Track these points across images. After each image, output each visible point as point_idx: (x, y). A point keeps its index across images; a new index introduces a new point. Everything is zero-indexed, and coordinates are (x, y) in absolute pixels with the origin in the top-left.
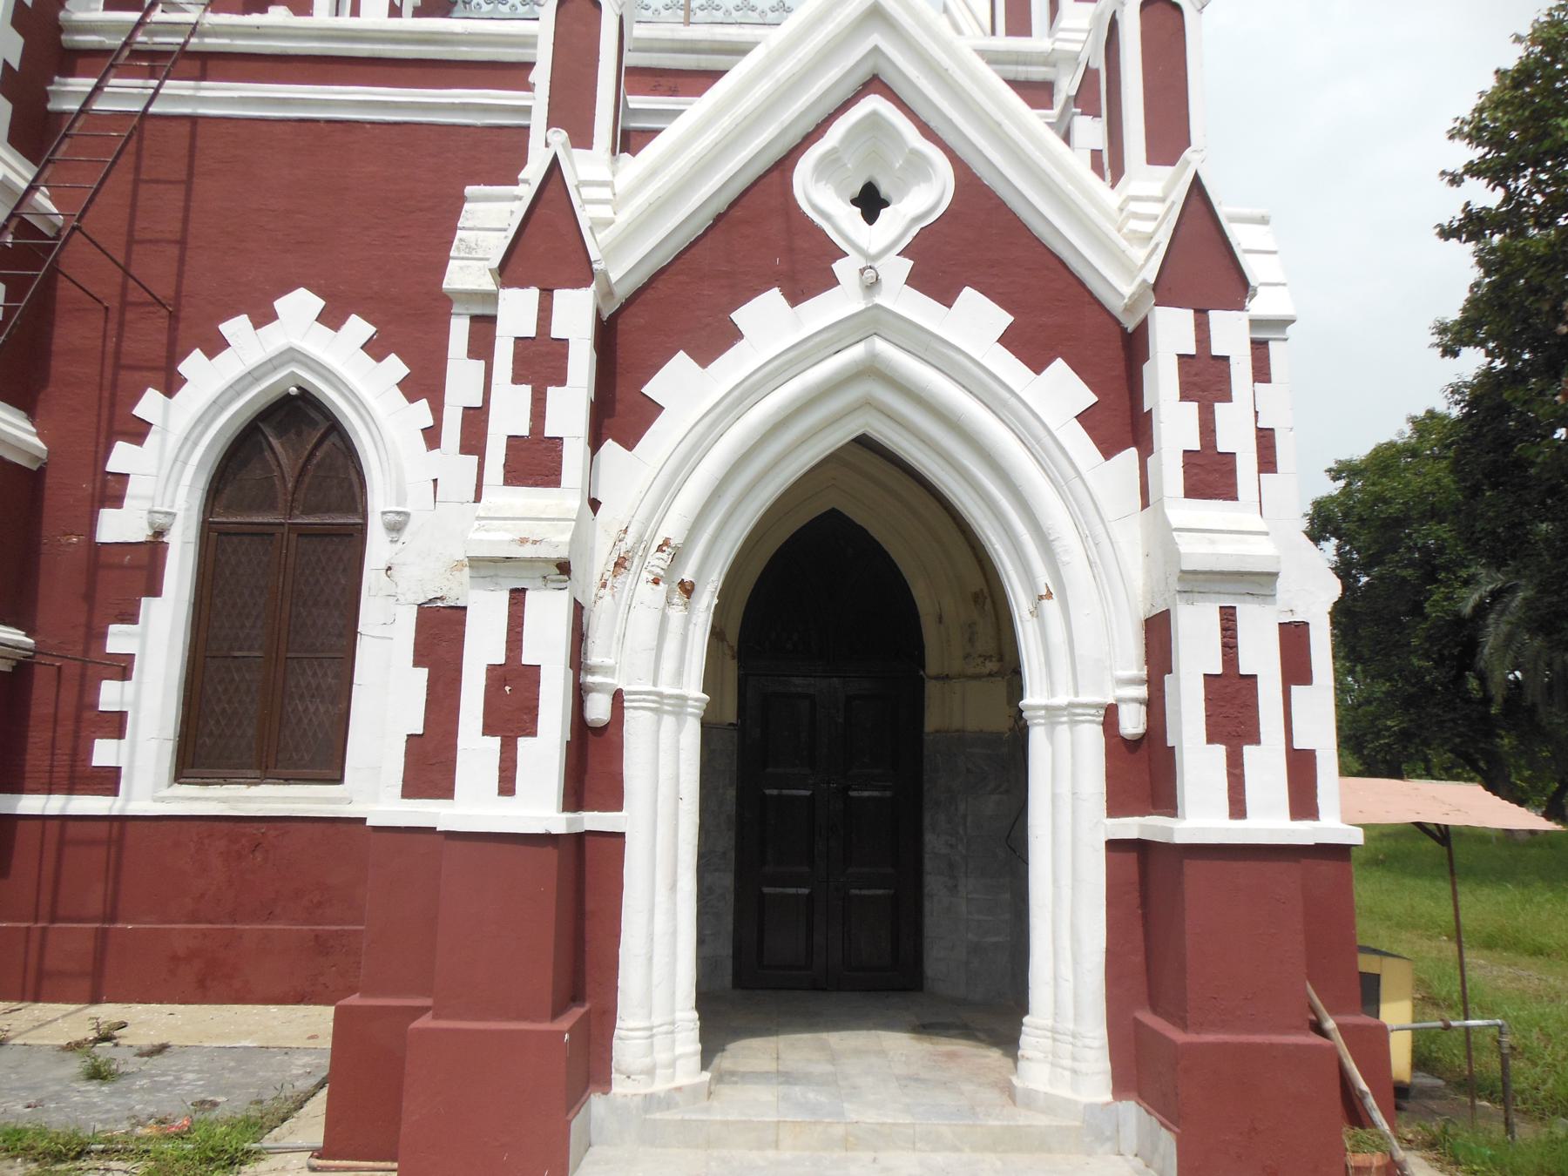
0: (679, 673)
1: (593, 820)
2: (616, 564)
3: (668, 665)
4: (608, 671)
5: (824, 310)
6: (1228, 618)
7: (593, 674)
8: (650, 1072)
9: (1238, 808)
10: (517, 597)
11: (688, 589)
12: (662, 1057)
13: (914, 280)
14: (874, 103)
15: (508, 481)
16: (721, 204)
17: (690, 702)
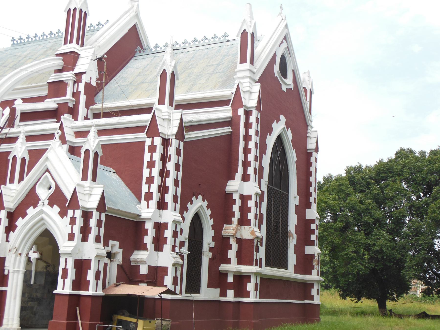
0: (19, 267)
2: (9, 251)
4: (7, 267)
6: (66, 259)
7: (6, 267)
8: (8, 325)
9: (63, 289)
11: (20, 254)
12: (10, 323)
13: (49, 204)
14: (47, 174)
17: (21, 271)
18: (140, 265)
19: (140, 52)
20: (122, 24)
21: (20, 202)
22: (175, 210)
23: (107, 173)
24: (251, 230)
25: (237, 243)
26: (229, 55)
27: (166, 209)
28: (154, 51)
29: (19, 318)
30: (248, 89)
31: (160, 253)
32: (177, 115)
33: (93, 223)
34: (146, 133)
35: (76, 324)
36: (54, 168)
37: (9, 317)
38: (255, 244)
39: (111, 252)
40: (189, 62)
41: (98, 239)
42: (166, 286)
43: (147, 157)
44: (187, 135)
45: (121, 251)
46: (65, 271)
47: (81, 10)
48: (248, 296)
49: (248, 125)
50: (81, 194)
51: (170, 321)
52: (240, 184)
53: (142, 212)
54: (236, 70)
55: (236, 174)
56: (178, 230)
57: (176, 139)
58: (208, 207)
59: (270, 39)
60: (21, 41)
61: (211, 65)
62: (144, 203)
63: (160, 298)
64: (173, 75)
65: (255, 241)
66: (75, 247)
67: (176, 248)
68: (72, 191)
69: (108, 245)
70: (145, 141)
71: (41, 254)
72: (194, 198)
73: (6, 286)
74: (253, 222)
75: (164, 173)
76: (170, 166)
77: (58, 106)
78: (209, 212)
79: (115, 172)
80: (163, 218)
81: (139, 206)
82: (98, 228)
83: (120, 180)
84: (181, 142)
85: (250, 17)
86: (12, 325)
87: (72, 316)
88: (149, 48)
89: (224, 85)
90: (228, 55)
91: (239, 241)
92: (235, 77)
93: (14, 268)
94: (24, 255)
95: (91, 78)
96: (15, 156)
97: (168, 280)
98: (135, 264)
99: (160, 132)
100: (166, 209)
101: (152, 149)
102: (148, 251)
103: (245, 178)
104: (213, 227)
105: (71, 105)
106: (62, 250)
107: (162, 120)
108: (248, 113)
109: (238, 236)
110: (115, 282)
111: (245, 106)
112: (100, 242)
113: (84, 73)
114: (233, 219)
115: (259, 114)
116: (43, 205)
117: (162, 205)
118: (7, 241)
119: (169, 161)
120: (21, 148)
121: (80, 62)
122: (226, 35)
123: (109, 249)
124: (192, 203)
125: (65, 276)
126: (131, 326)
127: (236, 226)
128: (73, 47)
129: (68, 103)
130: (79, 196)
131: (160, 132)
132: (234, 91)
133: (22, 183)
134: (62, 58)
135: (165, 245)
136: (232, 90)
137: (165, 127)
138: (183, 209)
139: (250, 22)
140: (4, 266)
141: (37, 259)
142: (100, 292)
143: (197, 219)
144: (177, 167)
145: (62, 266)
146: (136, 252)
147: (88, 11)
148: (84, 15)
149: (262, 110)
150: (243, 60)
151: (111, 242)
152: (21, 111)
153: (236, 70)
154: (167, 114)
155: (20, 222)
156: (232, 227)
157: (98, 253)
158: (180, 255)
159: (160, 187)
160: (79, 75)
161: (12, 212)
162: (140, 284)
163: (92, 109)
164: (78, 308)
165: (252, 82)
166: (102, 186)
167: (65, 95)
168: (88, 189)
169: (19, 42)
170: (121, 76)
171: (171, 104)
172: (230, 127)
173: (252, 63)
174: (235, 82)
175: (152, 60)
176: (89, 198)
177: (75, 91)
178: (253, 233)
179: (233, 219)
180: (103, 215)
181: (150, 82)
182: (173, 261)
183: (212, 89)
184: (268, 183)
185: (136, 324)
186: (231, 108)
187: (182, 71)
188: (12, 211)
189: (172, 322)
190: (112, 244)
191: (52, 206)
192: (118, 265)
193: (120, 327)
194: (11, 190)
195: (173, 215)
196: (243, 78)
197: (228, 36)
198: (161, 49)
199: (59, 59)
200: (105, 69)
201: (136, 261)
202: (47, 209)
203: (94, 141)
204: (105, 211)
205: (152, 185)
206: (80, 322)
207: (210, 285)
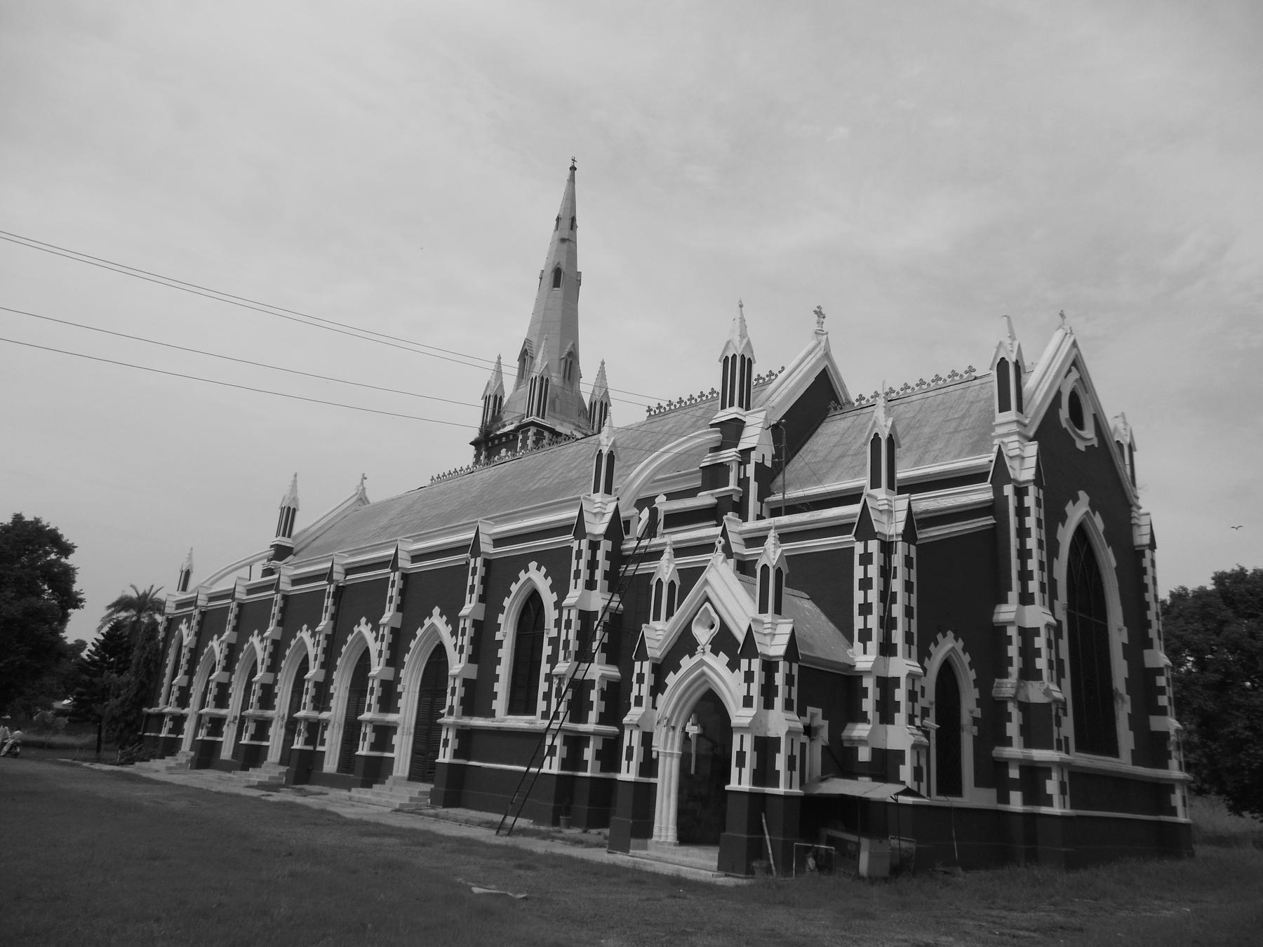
0: (672, 747)
1: (652, 780)
3: (669, 745)
5: (696, 659)
6: (742, 737)
8: (660, 836)
9: (740, 783)
10: (631, 731)
11: (674, 728)
12: (663, 833)
14: (707, 605)
15: (635, 706)
16: (679, 634)
18: (857, 748)
19: (835, 409)
20: (805, 369)
21: (669, 648)
22: (910, 657)
23: (796, 600)
24: (1044, 688)
25: (1020, 710)
26: (980, 401)
27: (895, 655)
28: (857, 406)
29: (675, 827)
30: (1017, 452)
31: (889, 726)
32: (901, 503)
33: (779, 679)
34: (855, 535)
35: (763, 840)
36: (717, 595)
37: (661, 824)
38: (1054, 713)
39: (812, 725)
40: (914, 417)
41: (788, 706)
42: (903, 783)
43: (858, 572)
44: (921, 533)
45: (826, 723)
46: (741, 755)
47: (743, 357)
48: (1050, 804)
49: (1022, 512)
50: (758, 635)
51: (913, 842)
52: (1018, 609)
53: (856, 660)
54: (994, 423)
55: (1009, 593)
56: (918, 689)
57: (902, 541)
58: (965, 650)
59: (1048, 367)
60: (660, 411)
61: (951, 419)
62: (858, 645)
63: (894, 801)
64: (891, 442)
65: (1054, 707)
66: (755, 717)
67: (916, 719)
68: (745, 629)
69: (805, 715)
70: (854, 548)
71: (703, 728)
72: (939, 636)
73: (656, 776)
74: (1045, 674)
75: (887, 597)
76: (897, 585)
77: (716, 501)
78: (966, 658)
79: (809, 597)
80: (890, 669)
81: (851, 650)
82: (787, 687)
83: (818, 610)
84: (911, 546)
85: (1010, 337)
86: (667, 836)
87: (755, 828)
88: (849, 402)
89: (975, 449)
90: (978, 400)
91: (1025, 707)
92: (993, 434)
93: (665, 749)
94: (679, 729)
95: (763, 455)
96: (660, 579)
97: (906, 772)
98: (849, 745)
99: (876, 531)
100: (895, 655)
101: (866, 559)
102: (869, 723)
103: (1026, 599)
104: (977, 683)
105: (736, 498)
106: (735, 722)
107: (879, 513)
108: (1021, 492)
109: (1022, 698)
110: (819, 774)
111: (1015, 481)
112: (792, 710)
113: (753, 449)
114: (1010, 669)
115: (1041, 491)
116: (704, 653)
117: (887, 649)
118: (654, 707)
119: (895, 577)
120: (667, 567)
121: (747, 432)
122: (971, 370)
123: (807, 720)
124: (936, 644)
125: (741, 764)
126: (849, 847)
127: (1015, 681)
128: (733, 412)
129: (732, 495)
130: (757, 638)
131: (876, 531)
132: (993, 457)
133: (673, 619)
134: (719, 429)
135: (896, 715)
136: (990, 456)
137: (884, 523)
138: (923, 656)
139: (1011, 344)
140: (651, 746)
141: (698, 736)
142: (796, 790)
143: (947, 669)
144: (908, 586)
145: (736, 748)
146: (849, 726)
147: (753, 357)
148: (747, 363)
149: (1044, 484)
150: (1004, 406)
151: (810, 710)
152: (665, 512)
153: (994, 423)
154: (886, 502)
155: (671, 679)
156: (1010, 683)
157: (790, 727)
158: (922, 731)
159: (882, 619)
160: (746, 453)
161: (659, 665)
162: (859, 778)
163: (768, 502)
164: (763, 815)
165: (1022, 440)
166: (792, 620)
167: (727, 485)
168: (769, 625)
169: (657, 411)
170: (809, 450)
171: (891, 485)
172: (991, 517)
173: (1020, 409)
174: (994, 443)
175: (855, 420)
176: (772, 639)
177: (742, 477)
178: (1047, 692)
179: (1010, 669)
180: (795, 667)
181: (855, 455)
182: (911, 739)
183: (955, 457)
184: (1066, 606)
185: (858, 845)
186: (990, 485)
187: (905, 433)
188: (659, 663)
189: (917, 844)
190: (811, 713)
191: (717, 655)
192: (822, 746)
193: (832, 849)
194: (656, 630)
195: (907, 664)
196: (1008, 435)
197: (974, 370)
198: (868, 401)
199: (716, 431)
200: (784, 440)
201: (851, 740)
202: (709, 658)
203: (774, 552)
204: (797, 660)
205: (869, 617)
206: (767, 837)
207: (979, 783)
